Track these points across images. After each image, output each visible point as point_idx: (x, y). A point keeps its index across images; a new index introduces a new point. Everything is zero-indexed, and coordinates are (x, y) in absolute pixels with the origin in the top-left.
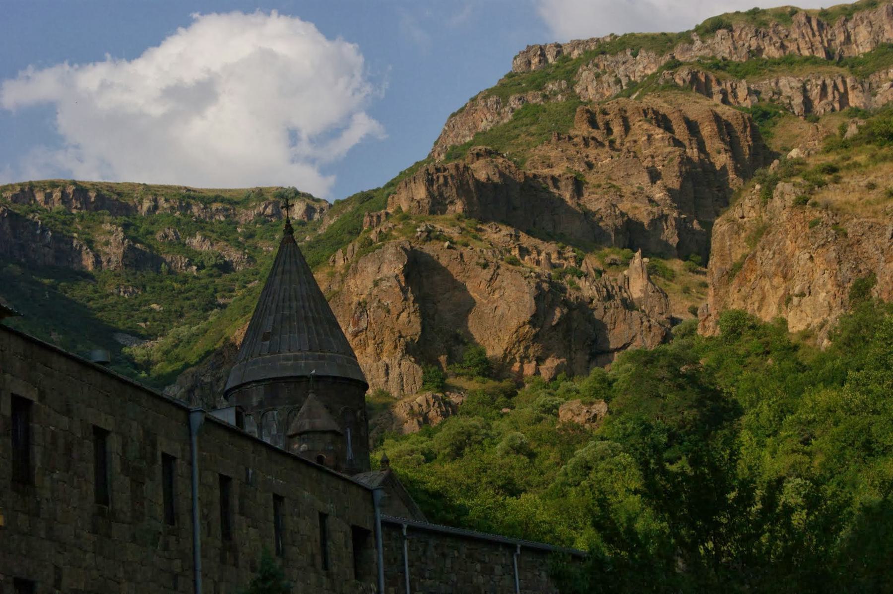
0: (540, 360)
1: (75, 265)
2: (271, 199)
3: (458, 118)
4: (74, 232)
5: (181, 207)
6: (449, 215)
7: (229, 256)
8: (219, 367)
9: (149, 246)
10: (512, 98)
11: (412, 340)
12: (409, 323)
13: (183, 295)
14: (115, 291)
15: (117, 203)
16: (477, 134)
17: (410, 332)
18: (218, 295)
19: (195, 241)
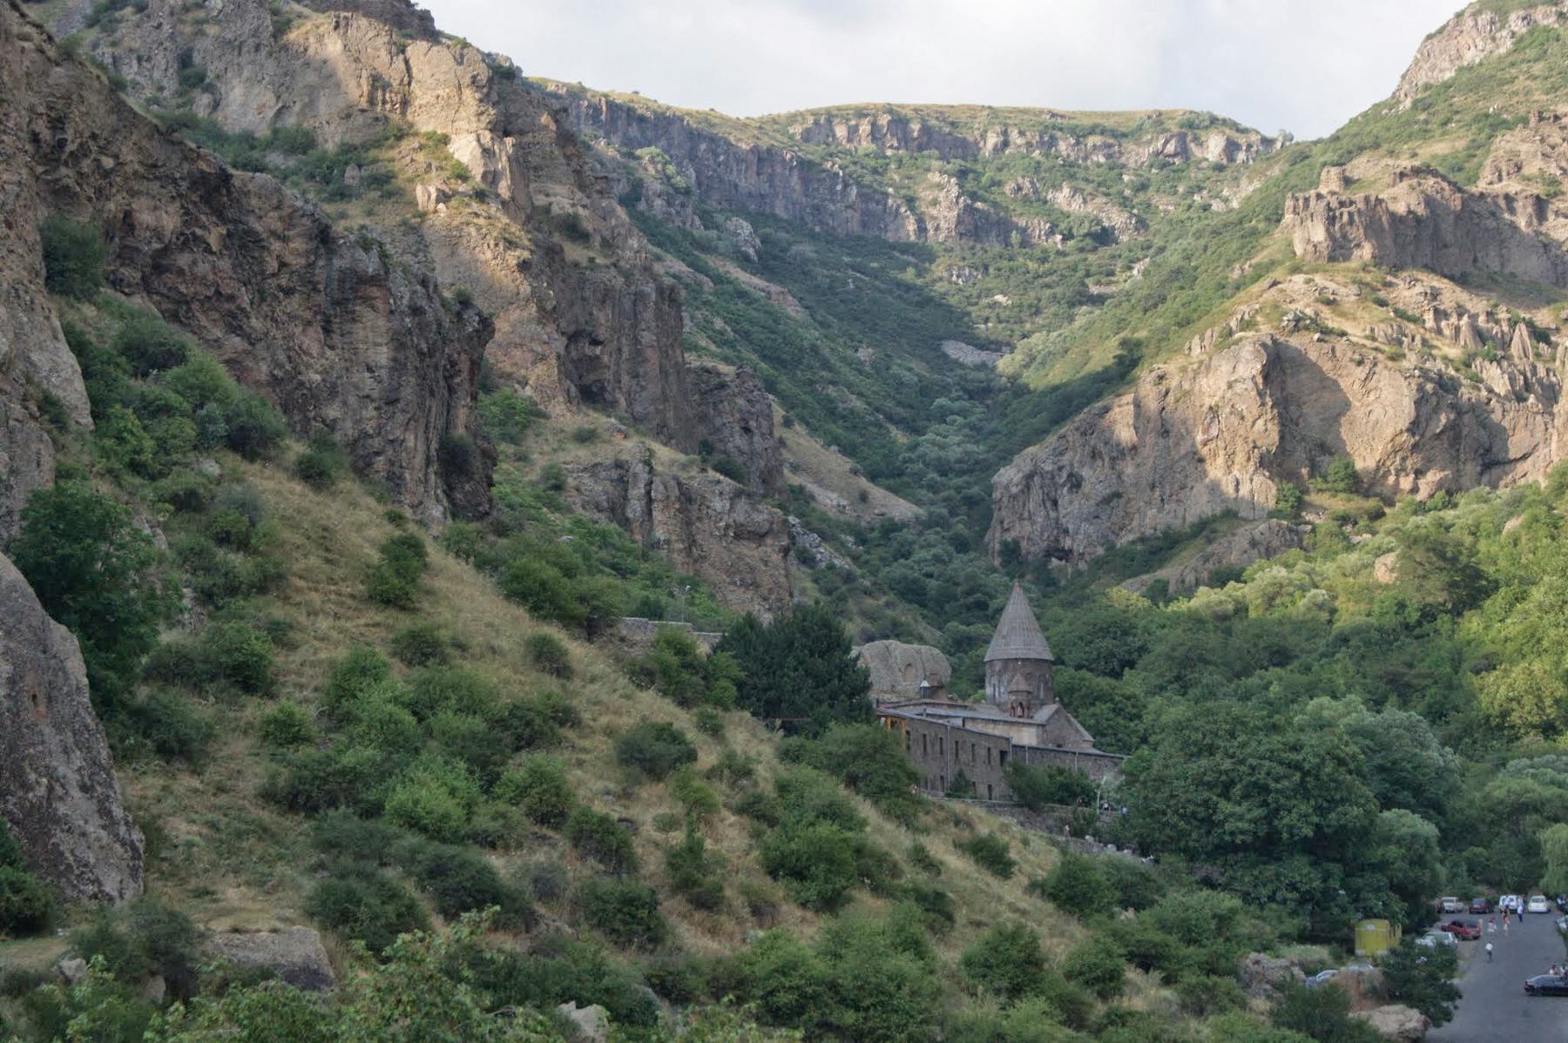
0: (1419, 473)
2: (1175, 130)
3: (1435, 41)
5: (1041, 143)
6: (1354, 264)
8: (1061, 454)
9: (995, 204)
10: (1513, 17)
12: (1266, 432)
14: (945, 275)
16: (1461, 69)
17: (1267, 442)
19: (1061, 197)
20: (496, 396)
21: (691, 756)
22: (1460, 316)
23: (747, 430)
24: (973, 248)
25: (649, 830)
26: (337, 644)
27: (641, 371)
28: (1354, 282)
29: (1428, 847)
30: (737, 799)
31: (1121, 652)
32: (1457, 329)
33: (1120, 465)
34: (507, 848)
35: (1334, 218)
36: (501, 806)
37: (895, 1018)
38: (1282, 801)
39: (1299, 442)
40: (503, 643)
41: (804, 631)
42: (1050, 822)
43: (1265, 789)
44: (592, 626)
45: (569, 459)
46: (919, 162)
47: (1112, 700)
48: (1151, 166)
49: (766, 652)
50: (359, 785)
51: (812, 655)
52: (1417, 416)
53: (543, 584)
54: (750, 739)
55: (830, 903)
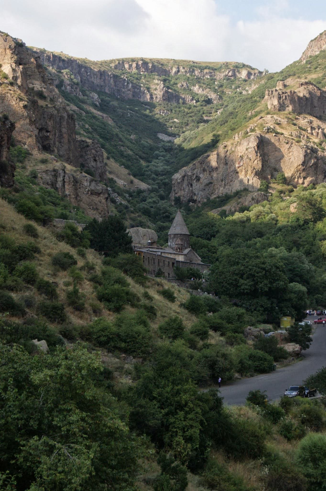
0: (305, 178)
1: (141, 99)
2: (232, 68)
3: (313, 42)
4: (142, 84)
5: (190, 71)
6: (286, 112)
7: (210, 96)
8: (194, 170)
9: (175, 90)
11: (258, 170)
12: (258, 164)
13: (189, 115)
14: (159, 112)
15: (161, 69)
17: (258, 167)
18: (204, 115)
19: (196, 89)
20: (16, 148)
21: (75, 263)
22: (319, 129)
23: (95, 160)
24: (168, 104)
25: (62, 286)
27: (62, 141)
28: (286, 118)
29: (304, 294)
30: (90, 276)
32: (318, 133)
35: (280, 97)
36: (15, 278)
37: (137, 345)
38: (259, 279)
40: (17, 227)
42: (187, 285)
43: (254, 276)
44: (45, 221)
45: (39, 168)
46: (151, 76)
47: (208, 247)
48: (224, 79)
52: (305, 160)
53: (29, 208)
54: (93, 257)
55: (118, 310)
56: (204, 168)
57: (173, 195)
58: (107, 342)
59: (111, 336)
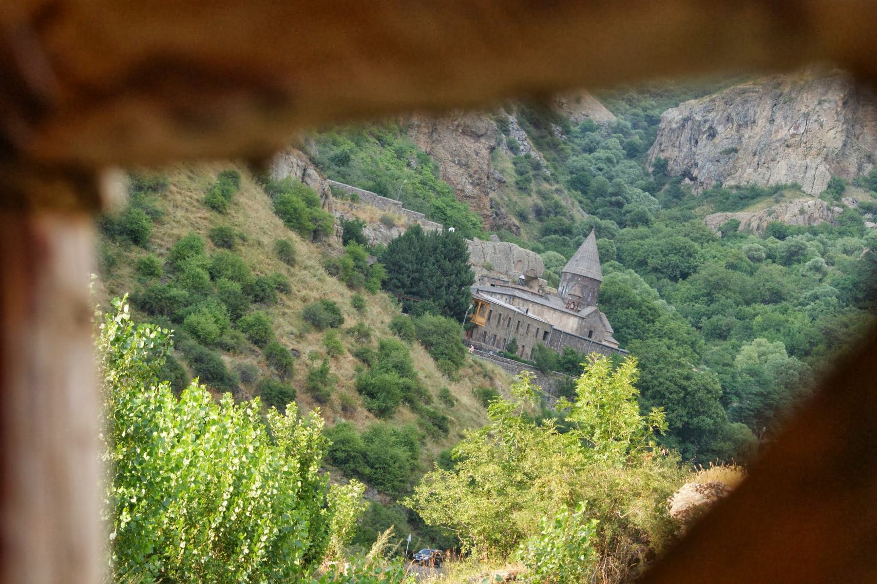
8: (709, 112)
21: (341, 321)
25: (305, 358)
26: (184, 226)
30: (358, 347)
31: (683, 266)
33: (743, 131)
34: (234, 353)
36: (238, 333)
37: (388, 476)
38: (670, 405)
39: (855, 151)
40: (266, 240)
41: (445, 245)
42: (551, 381)
44: (316, 234)
49: (421, 250)
50: (175, 306)
51: (445, 259)
53: (295, 210)
54: (380, 312)
55: (383, 413)
56: (730, 114)
57: (656, 152)
58: (345, 461)
59: (353, 454)
